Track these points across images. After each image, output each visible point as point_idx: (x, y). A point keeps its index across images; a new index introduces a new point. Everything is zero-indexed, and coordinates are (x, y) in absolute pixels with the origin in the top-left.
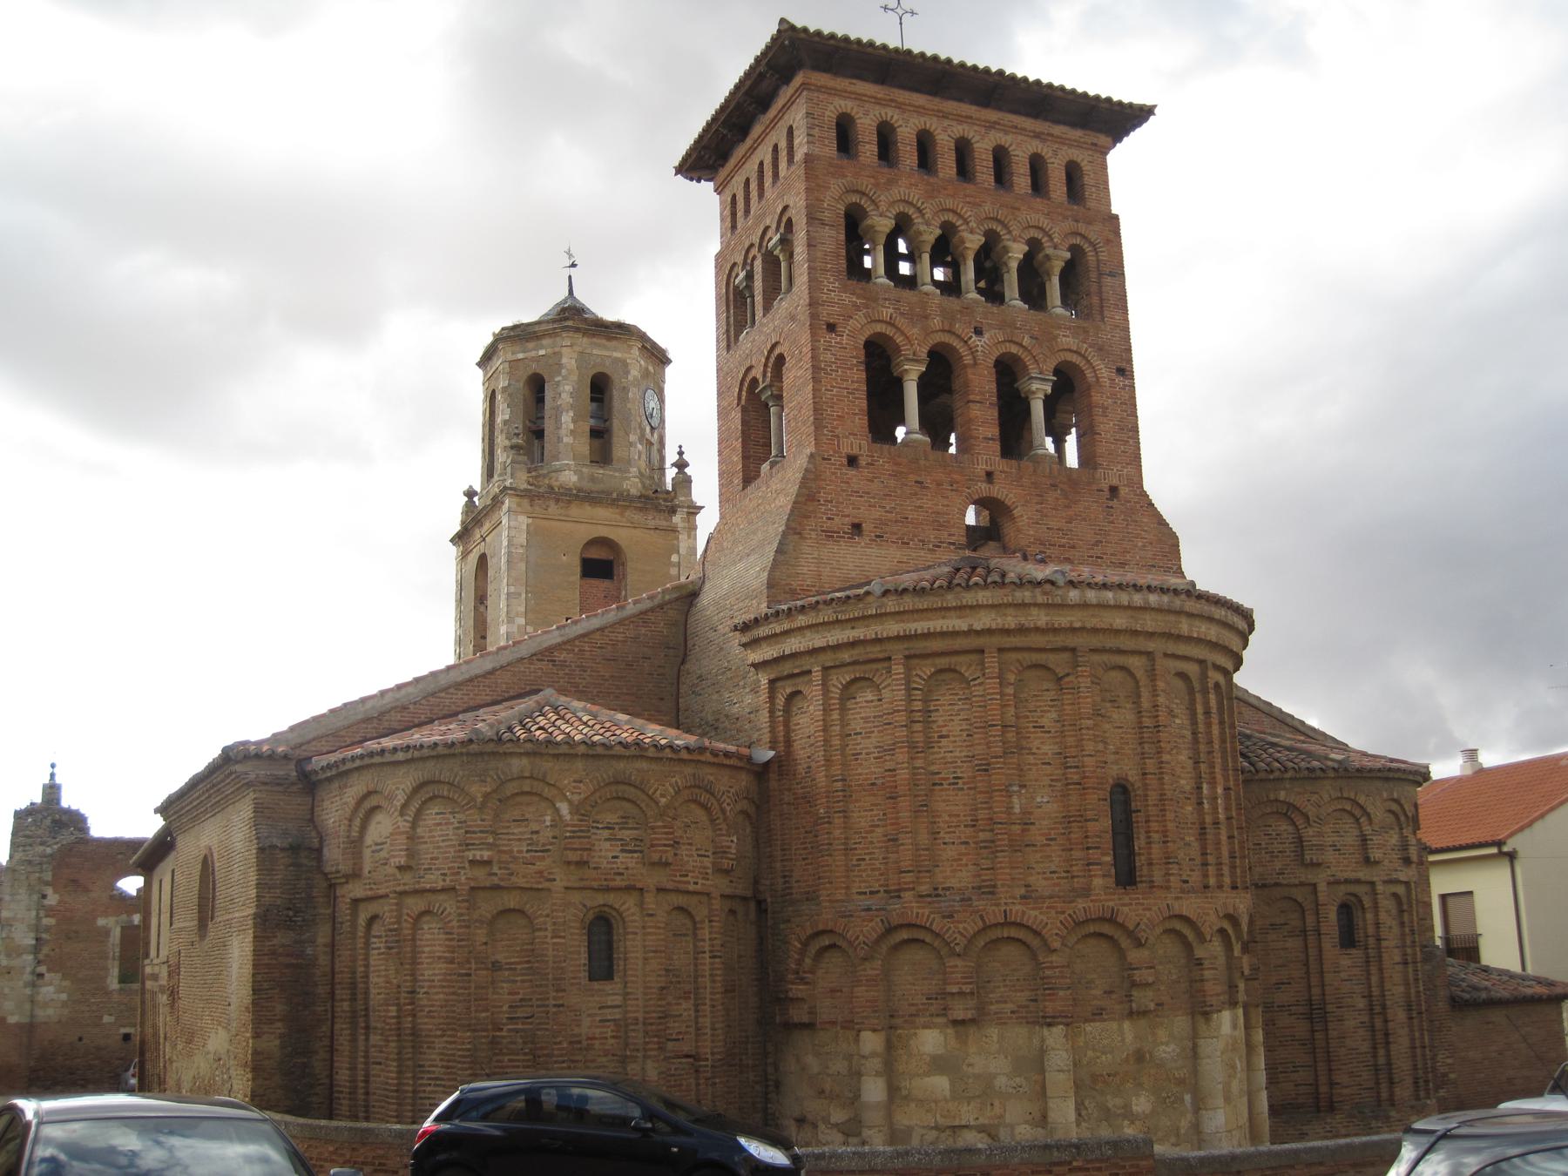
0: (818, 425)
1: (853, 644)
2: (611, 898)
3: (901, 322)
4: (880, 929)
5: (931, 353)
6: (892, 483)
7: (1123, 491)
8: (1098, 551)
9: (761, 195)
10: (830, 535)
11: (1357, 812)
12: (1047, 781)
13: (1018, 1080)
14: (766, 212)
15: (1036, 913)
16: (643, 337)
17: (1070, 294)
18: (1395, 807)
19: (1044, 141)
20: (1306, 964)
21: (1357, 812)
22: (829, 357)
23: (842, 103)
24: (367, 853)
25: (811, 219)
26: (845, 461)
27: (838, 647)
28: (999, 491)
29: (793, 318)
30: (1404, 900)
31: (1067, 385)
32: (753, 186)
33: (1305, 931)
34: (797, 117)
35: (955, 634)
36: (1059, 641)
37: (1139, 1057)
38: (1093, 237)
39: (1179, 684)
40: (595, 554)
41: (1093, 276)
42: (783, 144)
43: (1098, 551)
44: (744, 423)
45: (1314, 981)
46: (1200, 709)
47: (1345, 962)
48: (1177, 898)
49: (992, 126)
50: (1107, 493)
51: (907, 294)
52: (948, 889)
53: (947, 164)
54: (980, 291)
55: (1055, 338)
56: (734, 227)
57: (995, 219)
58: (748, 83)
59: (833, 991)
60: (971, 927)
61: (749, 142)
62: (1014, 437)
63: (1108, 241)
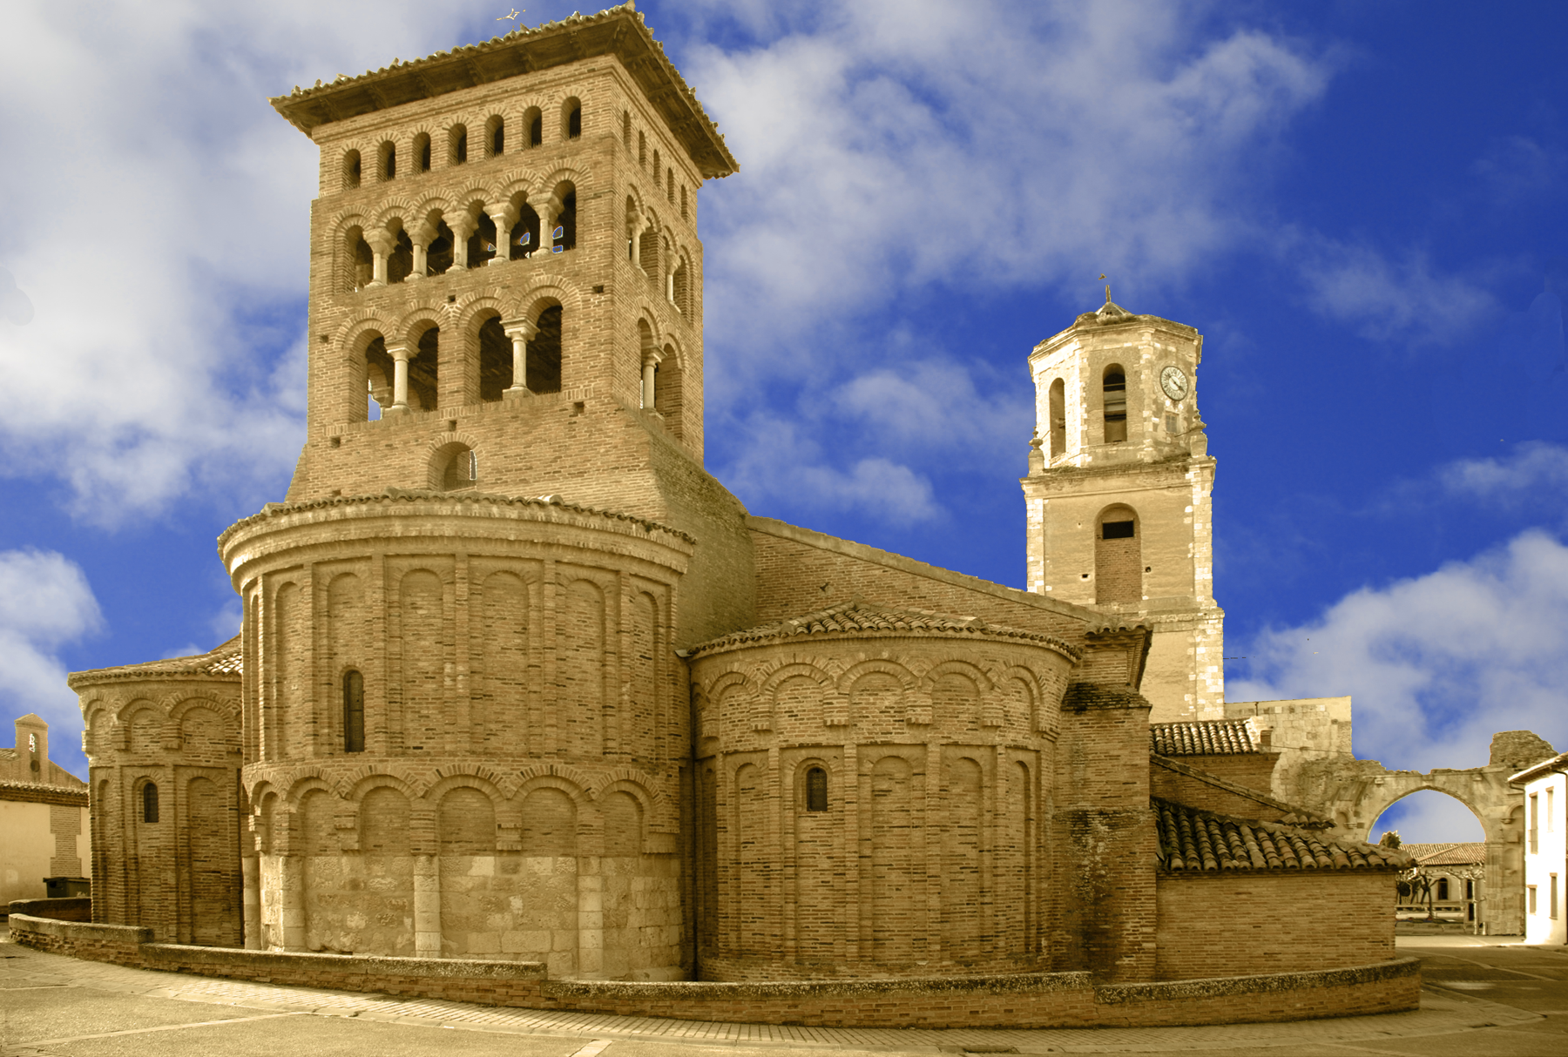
8: (555, 467)
17: (362, 252)
22: (322, 363)
23: (349, 142)
37: (355, 885)
43: (555, 467)
50: (571, 410)
57: (551, 177)
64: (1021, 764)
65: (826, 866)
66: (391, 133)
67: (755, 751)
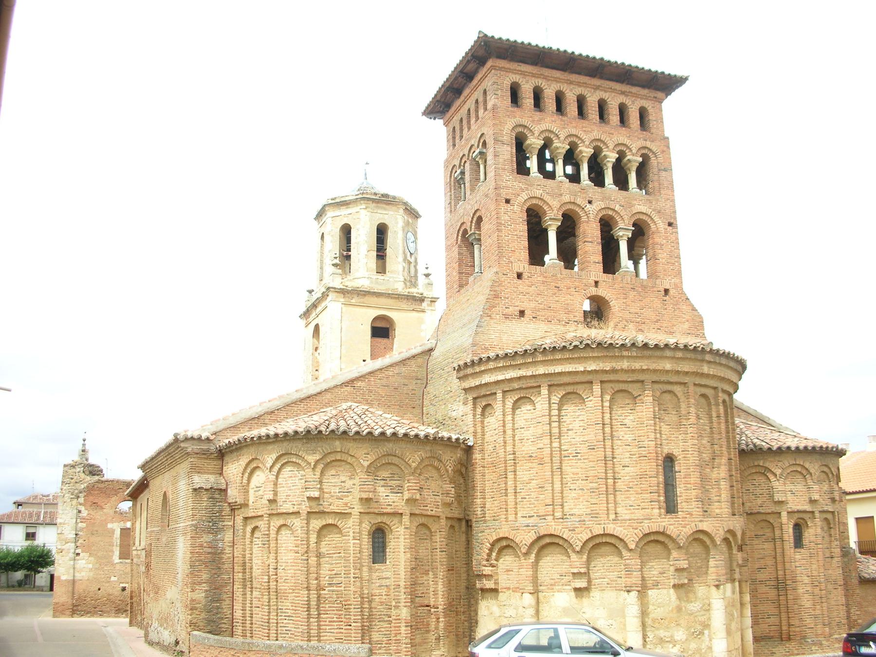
0: (500, 256)
1: (519, 378)
2: (385, 519)
3: (547, 198)
4: (534, 537)
5: (564, 215)
6: (542, 288)
7: (671, 292)
9: (469, 128)
10: (507, 317)
11: (804, 472)
12: (628, 455)
13: (610, 621)
14: (472, 136)
15: (621, 529)
16: (405, 204)
18: (826, 469)
19: (627, 96)
20: (775, 558)
21: (804, 472)
23: (514, 76)
24: (251, 492)
25: (496, 140)
26: (516, 276)
27: (511, 380)
28: (601, 292)
29: (487, 196)
30: (831, 522)
31: (640, 232)
32: (465, 122)
33: (774, 539)
34: (487, 84)
35: (576, 373)
36: (635, 377)
38: (654, 149)
39: (703, 400)
40: (379, 324)
41: (655, 170)
42: (481, 100)
44: (459, 254)
45: (780, 567)
46: (714, 414)
47: (798, 557)
48: (701, 521)
49: (597, 88)
50: (663, 293)
51: (550, 181)
52: (572, 515)
53: (572, 108)
54: (591, 179)
55: (633, 205)
56: (454, 145)
58: (462, 66)
59: (508, 571)
60: (585, 536)
61: (462, 98)
62: (610, 263)
63: (663, 151)
64: (826, 519)
65: (806, 581)
66: (564, 88)
67: (773, 513)
